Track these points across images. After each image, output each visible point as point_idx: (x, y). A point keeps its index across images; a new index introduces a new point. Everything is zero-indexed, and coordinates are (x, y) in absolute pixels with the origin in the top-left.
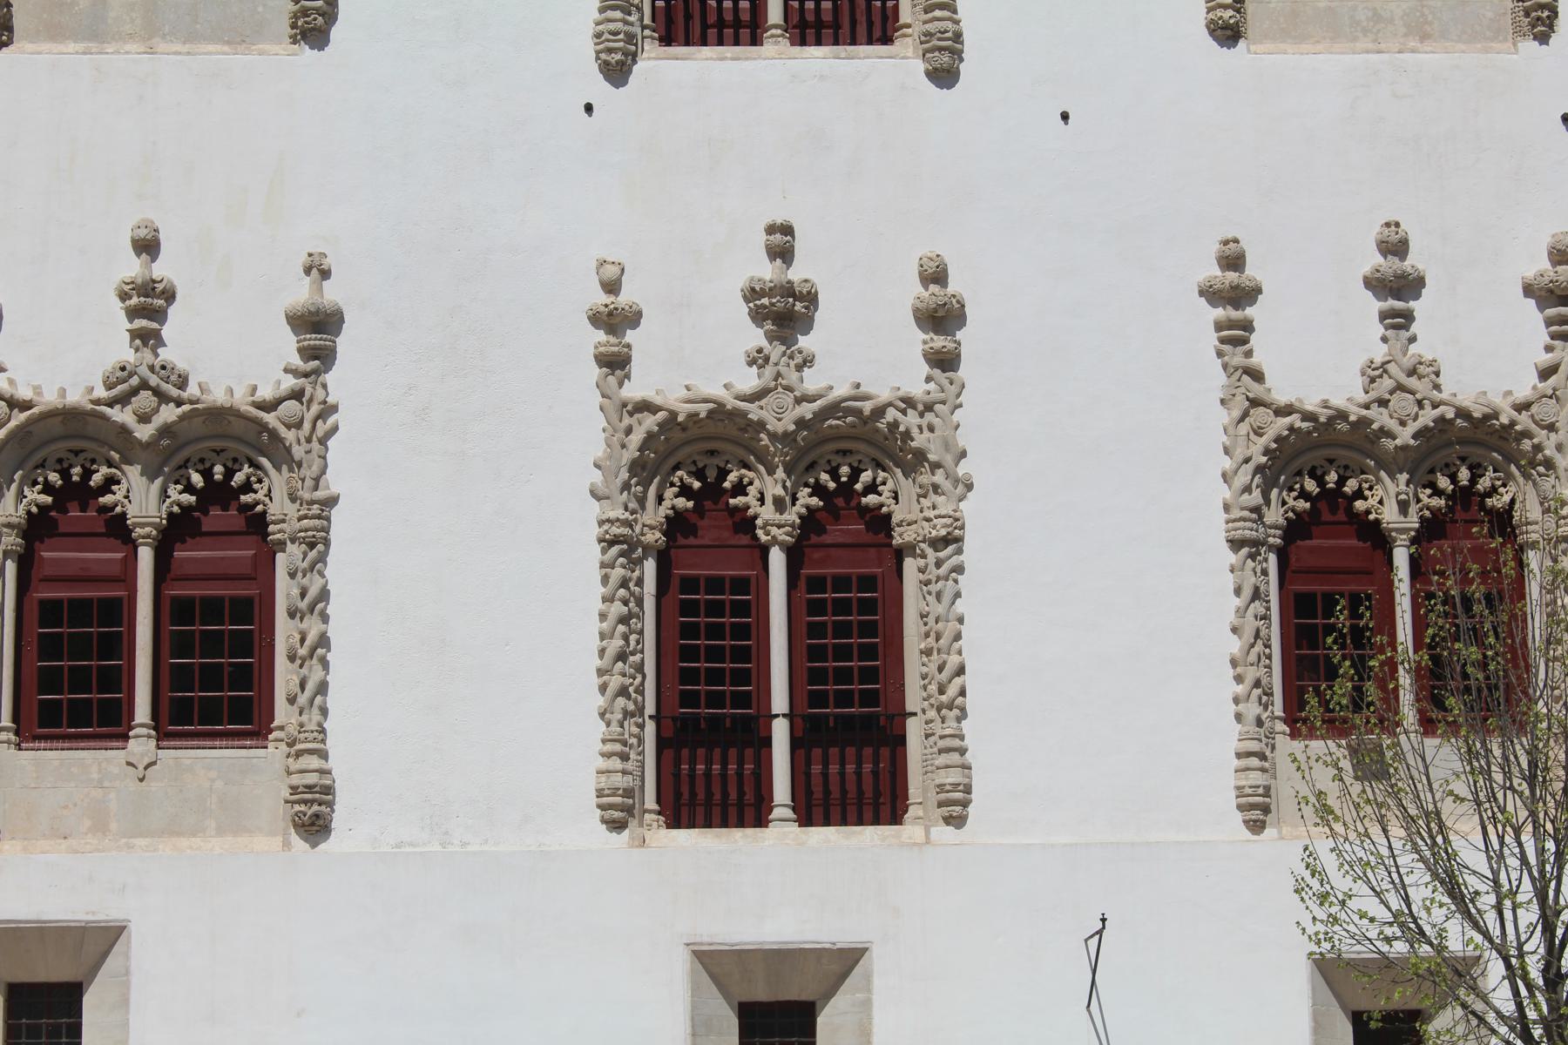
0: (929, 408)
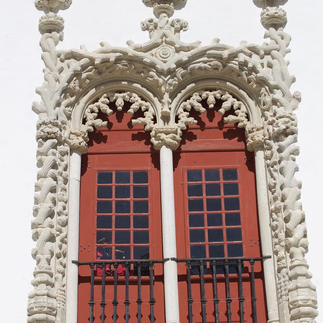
0: (268, 53)
